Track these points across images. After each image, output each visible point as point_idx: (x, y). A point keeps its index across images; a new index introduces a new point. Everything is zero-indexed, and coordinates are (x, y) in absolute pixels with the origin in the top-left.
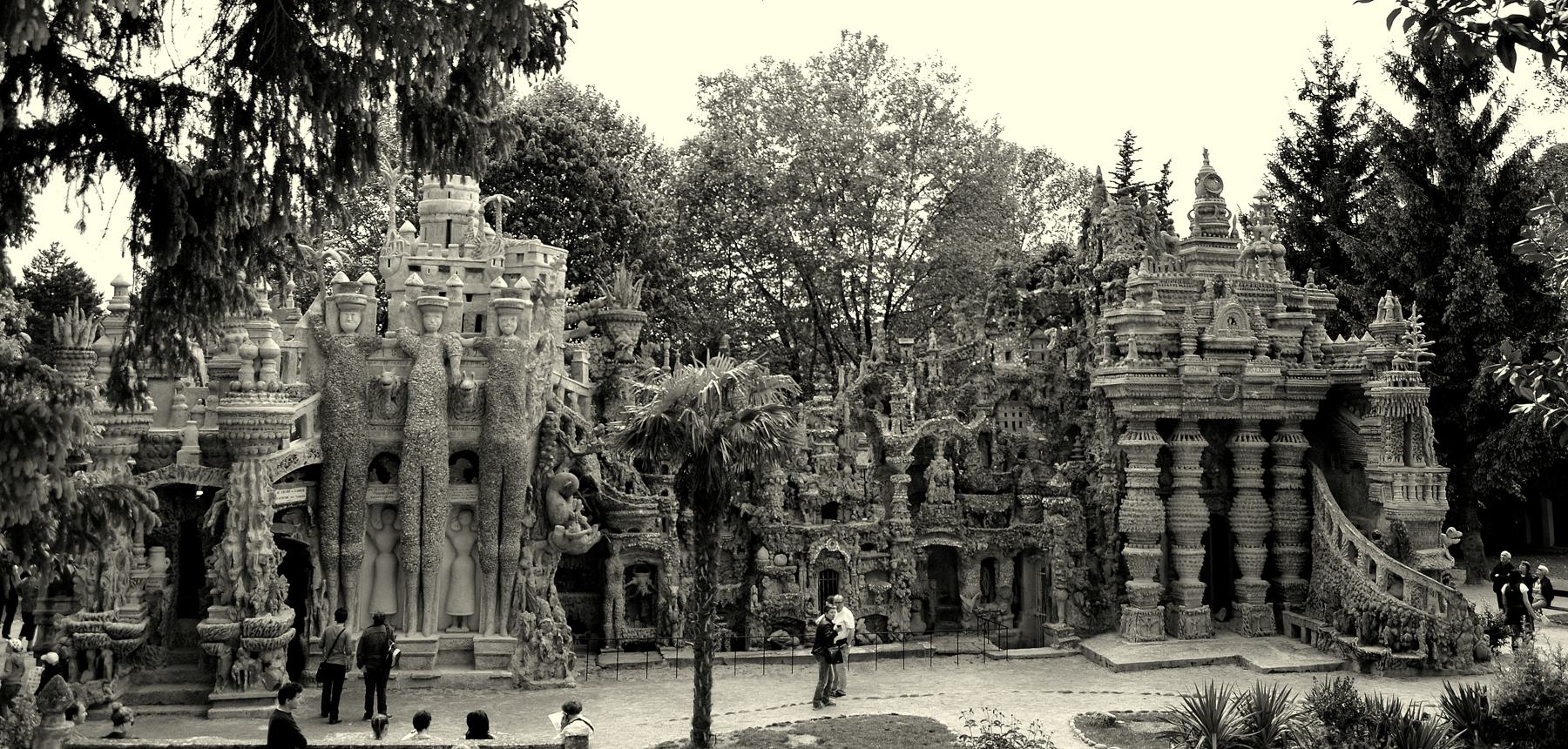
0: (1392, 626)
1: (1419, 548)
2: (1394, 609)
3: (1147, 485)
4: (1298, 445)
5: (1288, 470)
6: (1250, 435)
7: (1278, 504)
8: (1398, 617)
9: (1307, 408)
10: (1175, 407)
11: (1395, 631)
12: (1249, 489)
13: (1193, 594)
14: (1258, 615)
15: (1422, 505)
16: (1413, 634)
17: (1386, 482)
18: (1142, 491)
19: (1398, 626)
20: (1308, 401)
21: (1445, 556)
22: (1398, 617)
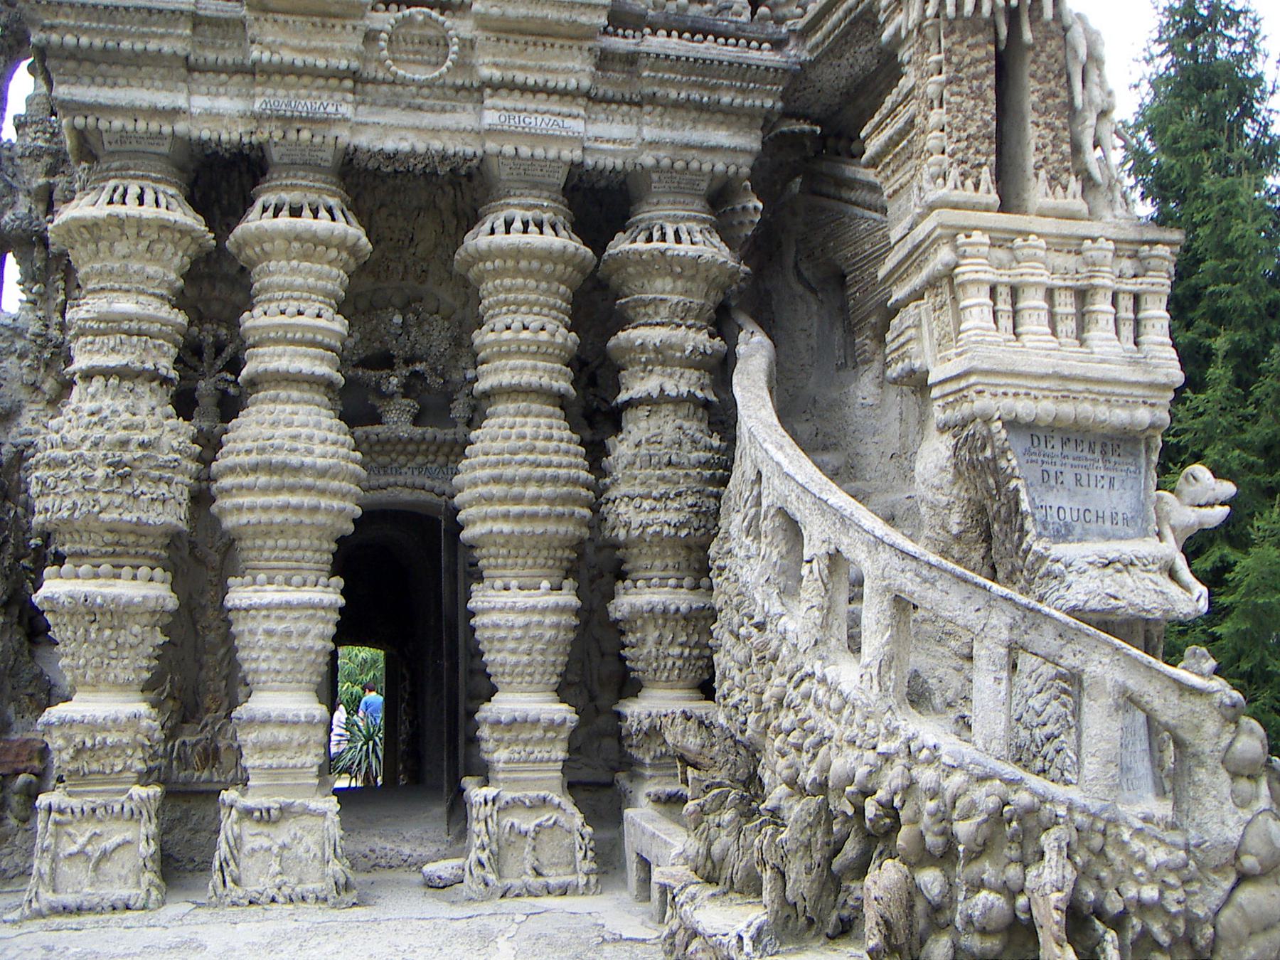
0: (922, 857)
1: (1065, 533)
2: (926, 776)
3: (114, 361)
4: (685, 248)
5: (655, 335)
6: (519, 215)
7: (622, 449)
8: (944, 817)
9: (720, 136)
10: (228, 104)
11: (931, 879)
12: (514, 392)
13: (275, 747)
14: (527, 822)
15: (1069, 358)
16: (1011, 892)
17: (932, 284)
18: (98, 383)
19: (946, 856)
20: (728, 116)
21: (1173, 575)
22: (944, 817)
